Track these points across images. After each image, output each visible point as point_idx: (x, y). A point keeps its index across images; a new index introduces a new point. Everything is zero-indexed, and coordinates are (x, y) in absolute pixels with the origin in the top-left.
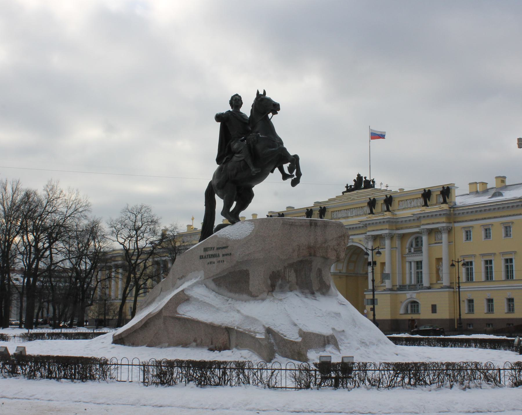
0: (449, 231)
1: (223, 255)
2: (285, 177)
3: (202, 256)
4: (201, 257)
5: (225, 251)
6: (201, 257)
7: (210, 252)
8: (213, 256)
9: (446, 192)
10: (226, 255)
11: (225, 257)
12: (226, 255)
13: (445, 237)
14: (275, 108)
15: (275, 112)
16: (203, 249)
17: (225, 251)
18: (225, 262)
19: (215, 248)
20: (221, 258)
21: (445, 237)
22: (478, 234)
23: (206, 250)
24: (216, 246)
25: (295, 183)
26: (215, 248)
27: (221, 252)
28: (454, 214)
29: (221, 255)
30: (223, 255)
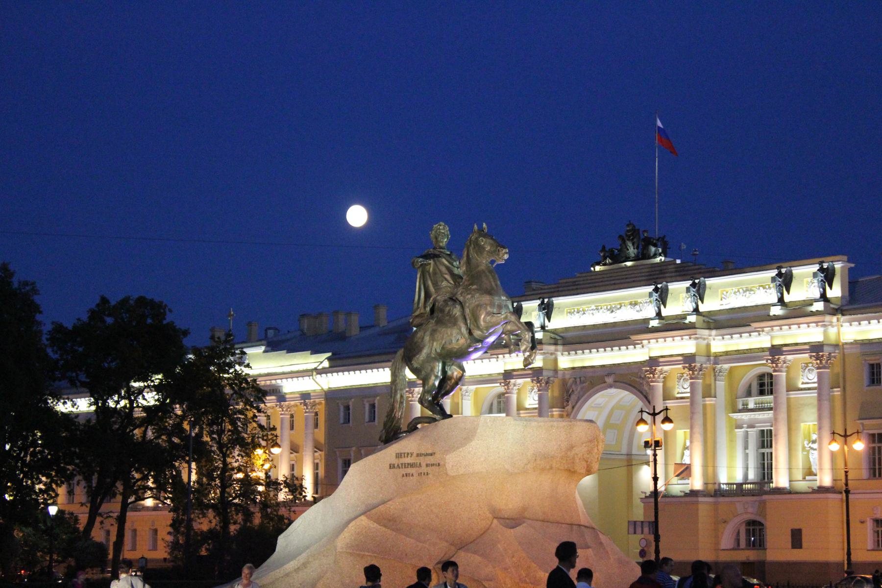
1: (427, 465)
3: (394, 465)
4: (392, 466)
5: (430, 460)
8: (412, 465)
10: (432, 465)
11: (429, 469)
12: (432, 465)
17: (430, 460)
18: (430, 476)
20: (424, 469)
23: (399, 456)
26: (415, 455)
27: (424, 461)
29: (424, 465)
30: (427, 465)
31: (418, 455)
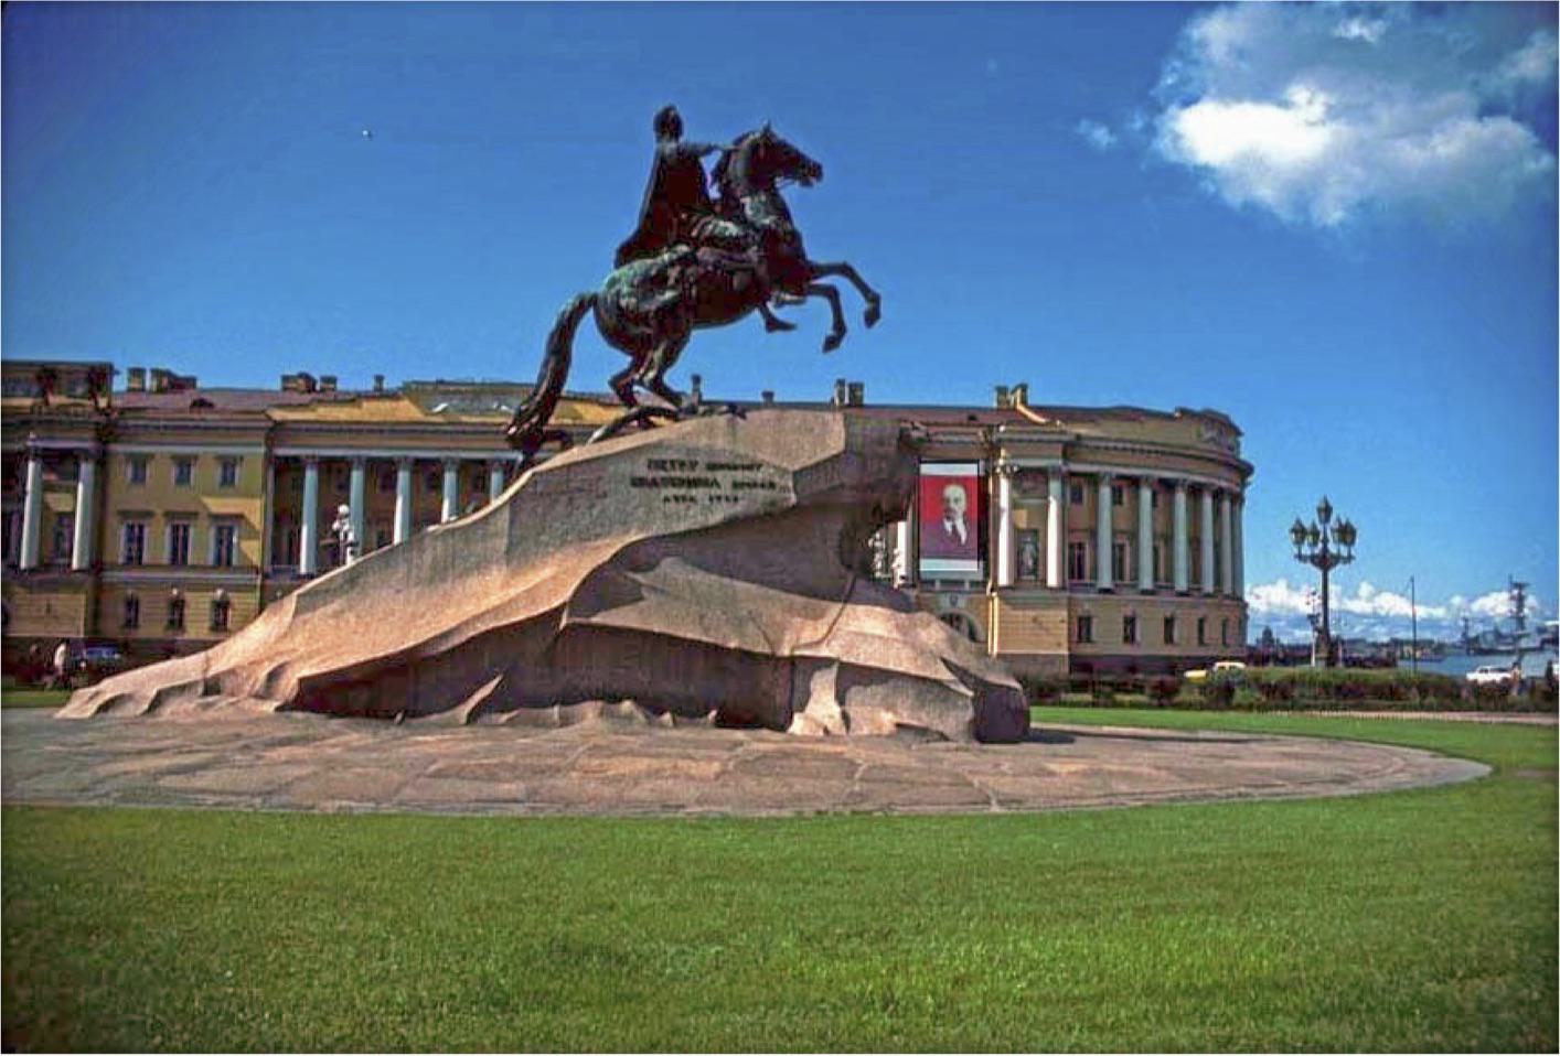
0: (102, 462)
1: (736, 485)
2: (773, 324)
4: (638, 482)
6: (638, 482)
7: (677, 474)
9: (98, 377)
13: (86, 469)
14: (806, 171)
15: (806, 183)
16: (643, 460)
19: (701, 465)
20: (726, 490)
21: (86, 469)
22: (161, 472)
24: (702, 460)
25: (831, 344)
26: (701, 465)
28: (109, 429)
31: (712, 467)
